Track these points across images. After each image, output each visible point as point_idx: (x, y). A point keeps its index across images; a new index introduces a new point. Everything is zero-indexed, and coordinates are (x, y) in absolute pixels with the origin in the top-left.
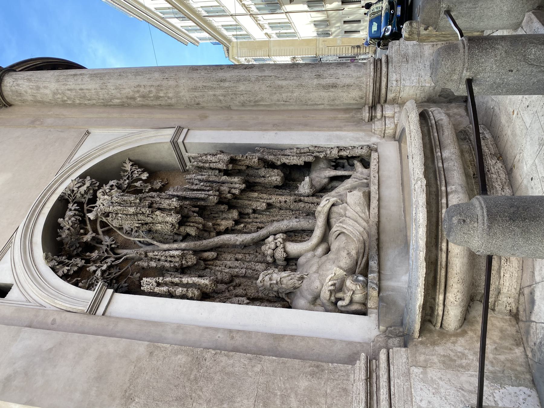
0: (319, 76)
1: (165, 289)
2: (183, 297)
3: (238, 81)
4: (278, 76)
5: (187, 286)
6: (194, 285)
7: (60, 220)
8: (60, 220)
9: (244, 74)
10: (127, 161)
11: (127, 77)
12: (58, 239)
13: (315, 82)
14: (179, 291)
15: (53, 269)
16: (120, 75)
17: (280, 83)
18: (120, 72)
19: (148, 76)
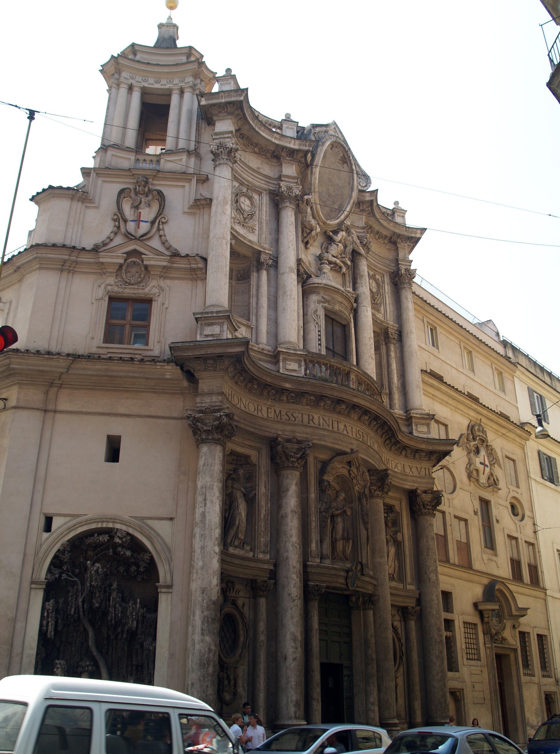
0: (192, 684)
1: (46, 614)
2: (41, 625)
3: (193, 626)
4: (195, 655)
5: (47, 625)
6: (47, 629)
7: (96, 535)
8: (96, 535)
9: (197, 630)
10: (150, 555)
11: (201, 541)
12: (84, 539)
13: (190, 683)
14: (45, 622)
15: (59, 551)
16: (202, 535)
17: (190, 657)
18: (205, 534)
19: (200, 557)
